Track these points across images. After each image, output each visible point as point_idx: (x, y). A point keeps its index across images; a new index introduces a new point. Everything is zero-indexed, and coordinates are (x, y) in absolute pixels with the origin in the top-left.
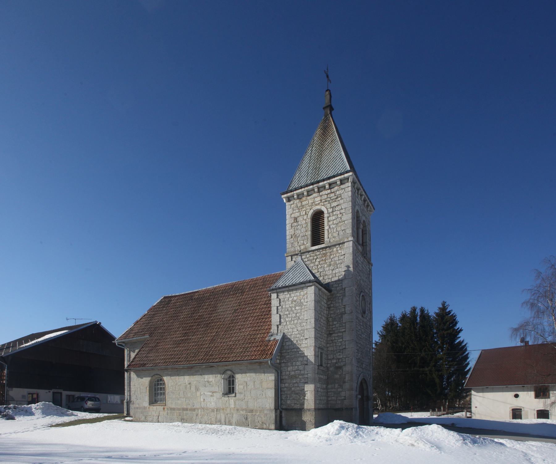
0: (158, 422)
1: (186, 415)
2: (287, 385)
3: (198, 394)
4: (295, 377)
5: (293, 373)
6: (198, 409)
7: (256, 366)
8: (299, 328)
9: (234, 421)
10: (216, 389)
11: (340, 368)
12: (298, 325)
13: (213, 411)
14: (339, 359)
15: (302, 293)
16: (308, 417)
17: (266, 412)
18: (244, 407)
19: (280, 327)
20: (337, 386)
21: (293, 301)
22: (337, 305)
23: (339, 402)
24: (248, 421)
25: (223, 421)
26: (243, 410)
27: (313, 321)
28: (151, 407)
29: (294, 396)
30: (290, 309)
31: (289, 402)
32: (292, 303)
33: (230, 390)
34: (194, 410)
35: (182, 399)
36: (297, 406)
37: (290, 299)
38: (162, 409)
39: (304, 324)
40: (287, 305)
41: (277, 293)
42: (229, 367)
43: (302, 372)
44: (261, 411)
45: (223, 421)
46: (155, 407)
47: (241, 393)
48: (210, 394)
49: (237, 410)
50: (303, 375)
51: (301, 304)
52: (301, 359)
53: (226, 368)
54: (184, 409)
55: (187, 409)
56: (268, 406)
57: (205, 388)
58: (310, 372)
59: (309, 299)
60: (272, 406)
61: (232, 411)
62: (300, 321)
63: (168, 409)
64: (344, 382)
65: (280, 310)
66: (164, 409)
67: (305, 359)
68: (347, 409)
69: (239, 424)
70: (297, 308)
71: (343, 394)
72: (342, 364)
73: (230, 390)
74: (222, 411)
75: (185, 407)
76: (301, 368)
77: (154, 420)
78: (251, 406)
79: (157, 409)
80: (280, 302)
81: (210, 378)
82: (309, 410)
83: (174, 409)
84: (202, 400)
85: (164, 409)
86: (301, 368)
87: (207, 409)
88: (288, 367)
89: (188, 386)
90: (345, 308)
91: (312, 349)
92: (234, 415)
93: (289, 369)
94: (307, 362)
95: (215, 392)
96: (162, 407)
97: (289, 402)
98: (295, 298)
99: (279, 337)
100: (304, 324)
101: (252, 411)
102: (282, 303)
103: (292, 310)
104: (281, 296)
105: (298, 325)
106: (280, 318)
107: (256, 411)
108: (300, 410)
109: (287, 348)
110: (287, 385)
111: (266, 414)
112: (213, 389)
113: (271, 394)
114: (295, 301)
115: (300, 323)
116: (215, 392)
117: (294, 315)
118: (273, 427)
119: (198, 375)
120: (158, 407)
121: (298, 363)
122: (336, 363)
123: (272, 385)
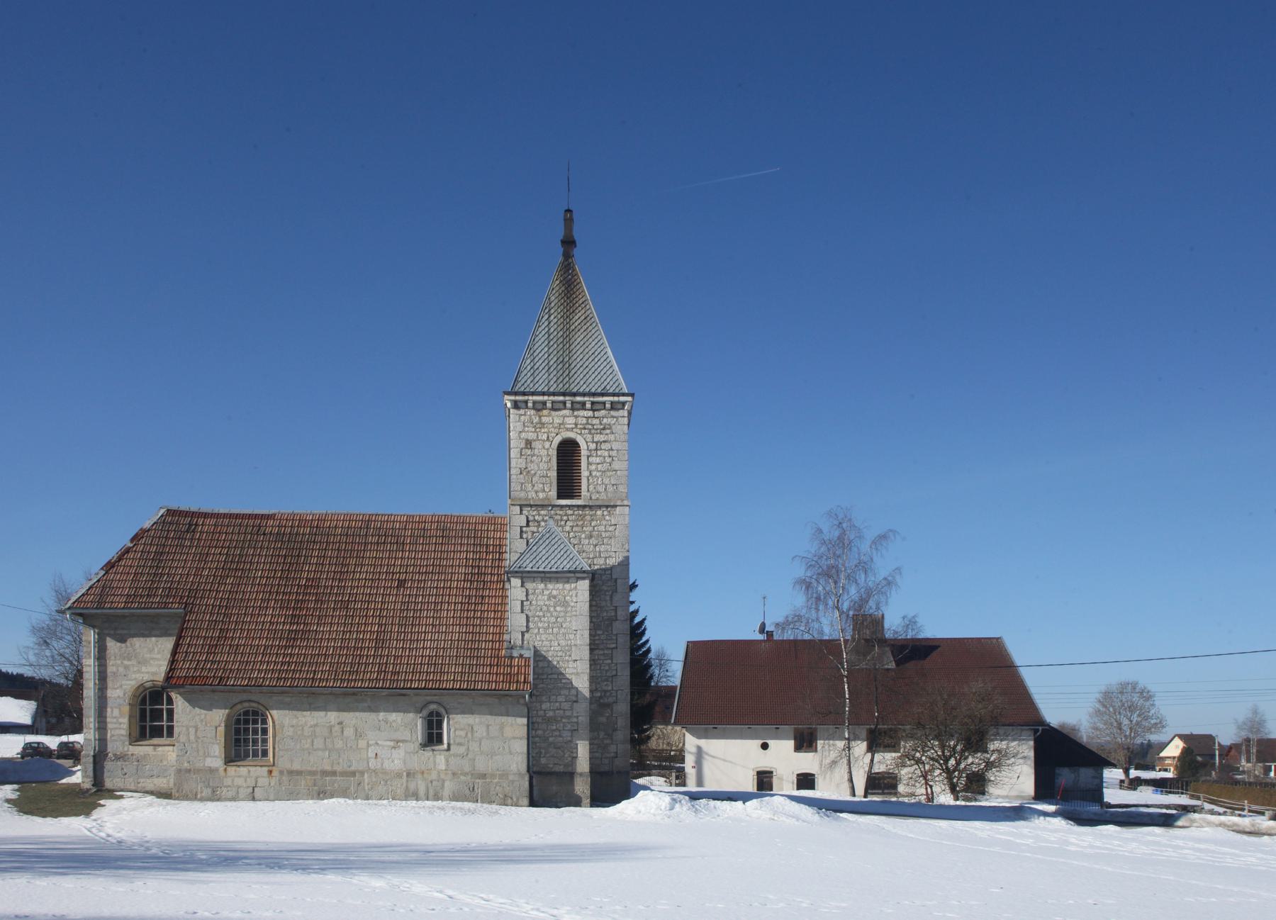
0: (254, 799)
1: (324, 784)
2: (540, 732)
3: (362, 744)
4: (554, 720)
5: (551, 714)
6: (362, 773)
7: (497, 698)
8: (563, 643)
9: (446, 792)
10: (406, 735)
11: (608, 705)
12: (560, 637)
13: (399, 775)
14: (606, 691)
15: (567, 586)
16: (582, 787)
17: (511, 778)
18: (467, 769)
19: (527, 636)
20: (602, 735)
21: (550, 597)
22: (603, 604)
23: (606, 761)
24: (476, 789)
25: (422, 792)
26: (465, 774)
27: (587, 634)
28: (232, 770)
29: (553, 751)
30: (545, 608)
31: (543, 761)
32: (549, 599)
33: (433, 737)
34: (353, 774)
35: (320, 753)
36: (560, 769)
37: (546, 592)
38: (266, 774)
39: (572, 637)
40: (542, 600)
41: (522, 578)
42: (435, 698)
43: (568, 713)
44: (501, 776)
45: (422, 792)
46: (243, 770)
47: (460, 744)
48: (392, 744)
49: (454, 774)
50: (569, 717)
51: (565, 604)
52: (566, 692)
53: (429, 698)
54: (325, 773)
55: (334, 773)
56: (514, 767)
57: (388, 736)
58: (582, 713)
59: (580, 598)
60: (523, 767)
61: (442, 776)
62: (563, 630)
63: (281, 772)
64: (615, 730)
65: (526, 608)
66: (270, 772)
67: (573, 692)
68: (619, 772)
69: (456, 797)
70: (558, 609)
71: (613, 748)
72: (611, 700)
73: (433, 737)
74: (420, 776)
75: (328, 768)
76: (566, 706)
77: (241, 796)
78: (481, 765)
79: (243, 774)
80: (527, 595)
81: (396, 717)
82: (581, 774)
83: (299, 773)
84: (372, 755)
85: (270, 772)
86: (566, 706)
87: (385, 773)
88: (541, 702)
89: (337, 728)
90: (616, 611)
91: (586, 677)
92: (447, 784)
93: (544, 706)
94: (576, 697)
95: (403, 741)
96: (266, 769)
97: (543, 761)
98: (554, 592)
99: (528, 654)
100: (572, 637)
101: (483, 776)
102: (530, 597)
103: (548, 611)
104: (530, 585)
105: (560, 637)
106: (528, 621)
107: (493, 776)
108: (570, 775)
109: (546, 674)
110: (540, 732)
111: (513, 782)
112: (398, 736)
113: (521, 747)
114: (555, 597)
115: (564, 634)
116: (403, 741)
117: (553, 619)
118: (526, 801)
119: (363, 710)
120: (252, 769)
121: (560, 699)
122: (601, 697)
123: (523, 732)
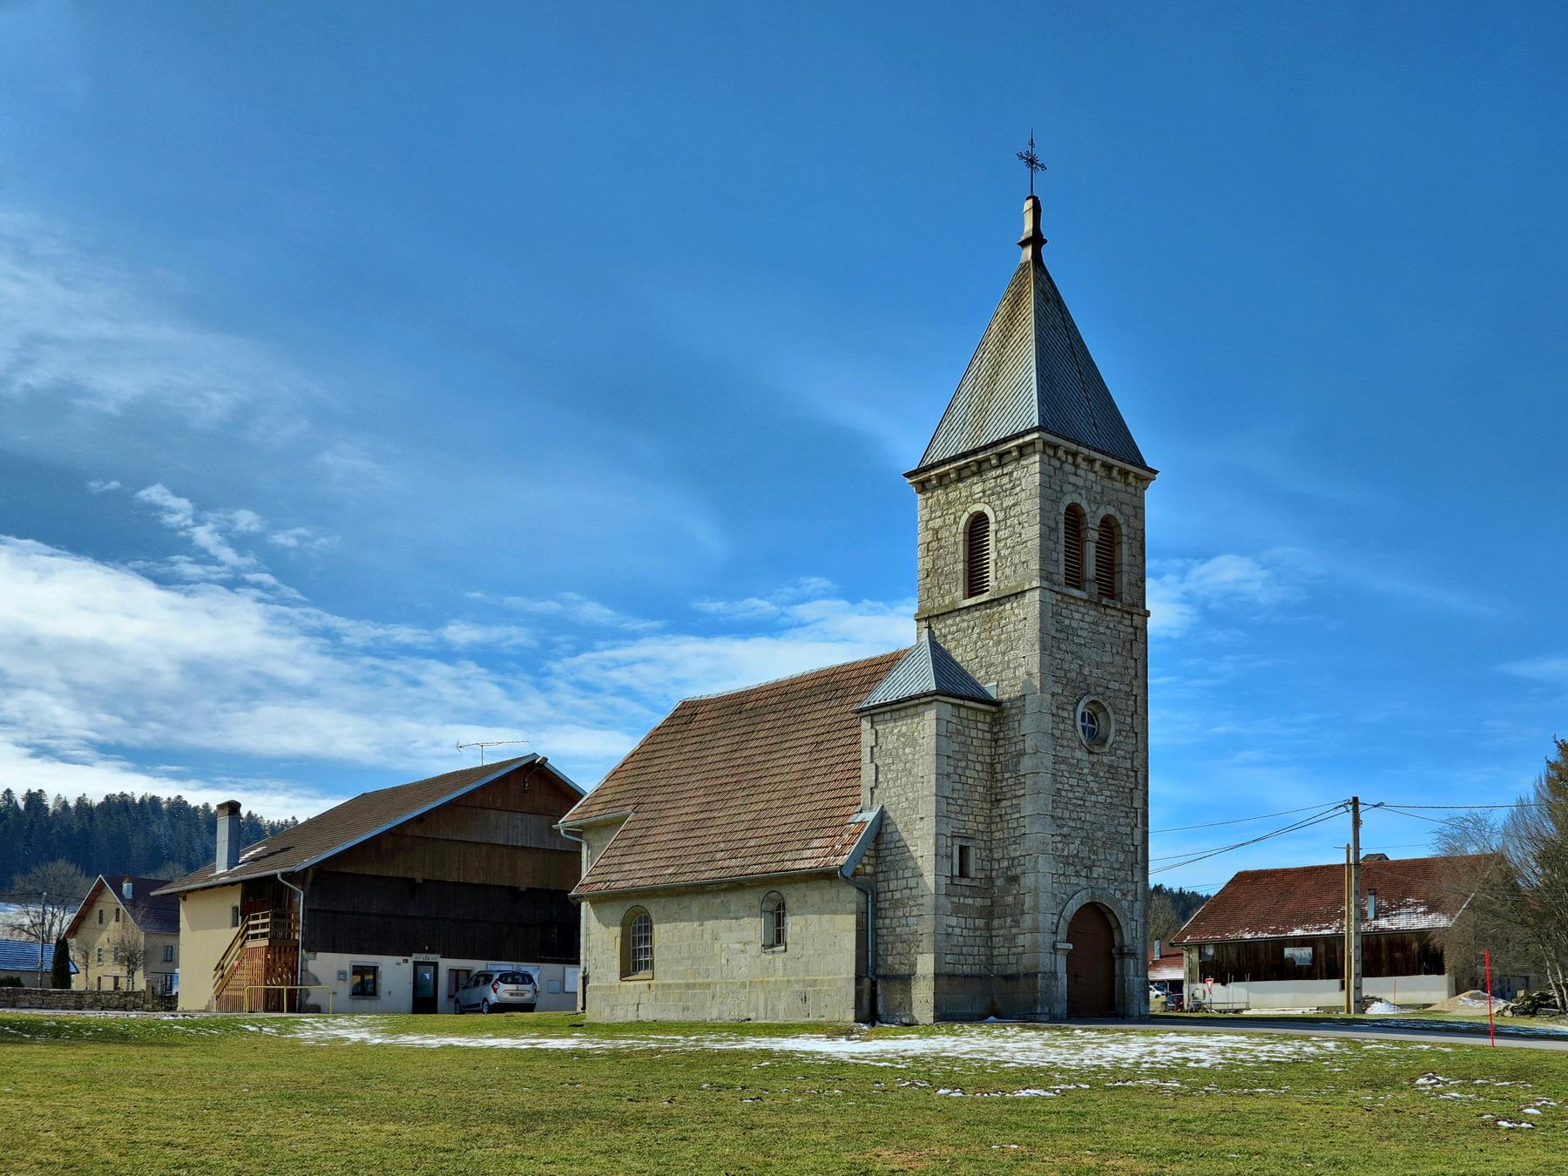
2: (887, 921)
13: (743, 985)
19: (876, 792)
22: (1011, 734)
33: (777, 938)
36: (904, 970)
40: (890, 742)
48: (739, 946)
64: (1023, 913)
68: (1026, 975)
71: (1021, 940)
72: (1019, 870)
73: (777, 938)
84: (724, 962)
97: (890, 959)
102: (881, 740)
114: (904, 735)
122: (1008, 868)
